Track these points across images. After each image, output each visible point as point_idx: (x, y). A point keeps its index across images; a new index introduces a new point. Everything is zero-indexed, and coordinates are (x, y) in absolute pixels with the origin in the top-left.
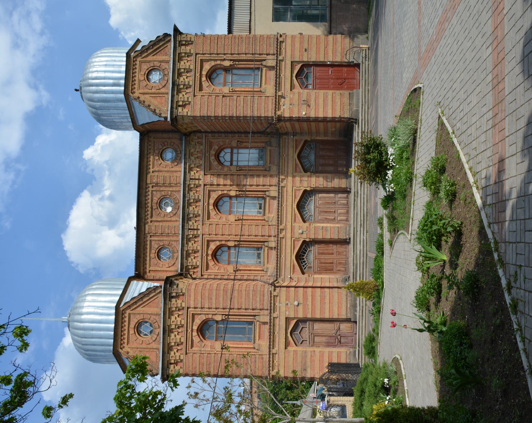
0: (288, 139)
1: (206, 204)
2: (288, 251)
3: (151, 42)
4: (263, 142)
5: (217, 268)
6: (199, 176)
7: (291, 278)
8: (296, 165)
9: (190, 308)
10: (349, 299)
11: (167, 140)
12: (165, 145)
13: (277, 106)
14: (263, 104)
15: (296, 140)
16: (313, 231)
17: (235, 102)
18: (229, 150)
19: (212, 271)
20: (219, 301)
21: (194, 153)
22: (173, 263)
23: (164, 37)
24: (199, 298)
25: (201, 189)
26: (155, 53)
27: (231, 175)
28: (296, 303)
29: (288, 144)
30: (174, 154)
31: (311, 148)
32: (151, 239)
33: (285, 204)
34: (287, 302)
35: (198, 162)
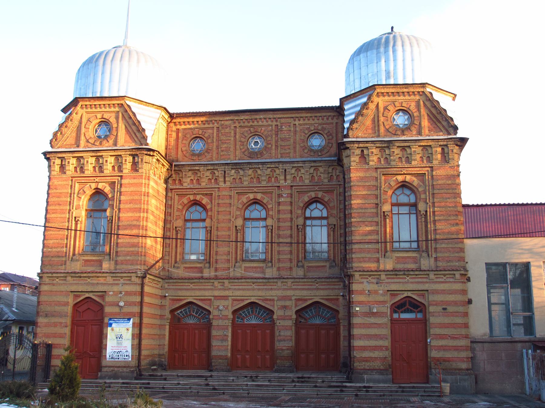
0: (339, 289)
1: (255, 190)
2: (198, 293)
3: (445, 110)
4: (334, 257)
5: (180, 207)
6: (288, 180)
7: (165, 296)
8: (306, 300)
9: (121, 179)
10: (125, 369)
11: (335, 139)
12: (328, 136)
13: (367, 273)
14: (369, 255)
15: (337, 299)
16: (221, 322)
17: (369, 219)
18: (325, 214)
19: (176, 201)
20: (128, 212)
21: (319, 172)
22: (187, 155)
23: (452, 126)
24: (132, 189)
25: (273, 183)
26: (432, 116)
27: (291, 219)
28: (122, 304)
29: (332, 289)
30: (316, 148)
31: (329, 320)
32: (215, 128)
33: (256, 287)
34: (123, 293)
35: (308, 177)
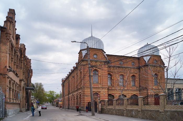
28: (104, 94)
